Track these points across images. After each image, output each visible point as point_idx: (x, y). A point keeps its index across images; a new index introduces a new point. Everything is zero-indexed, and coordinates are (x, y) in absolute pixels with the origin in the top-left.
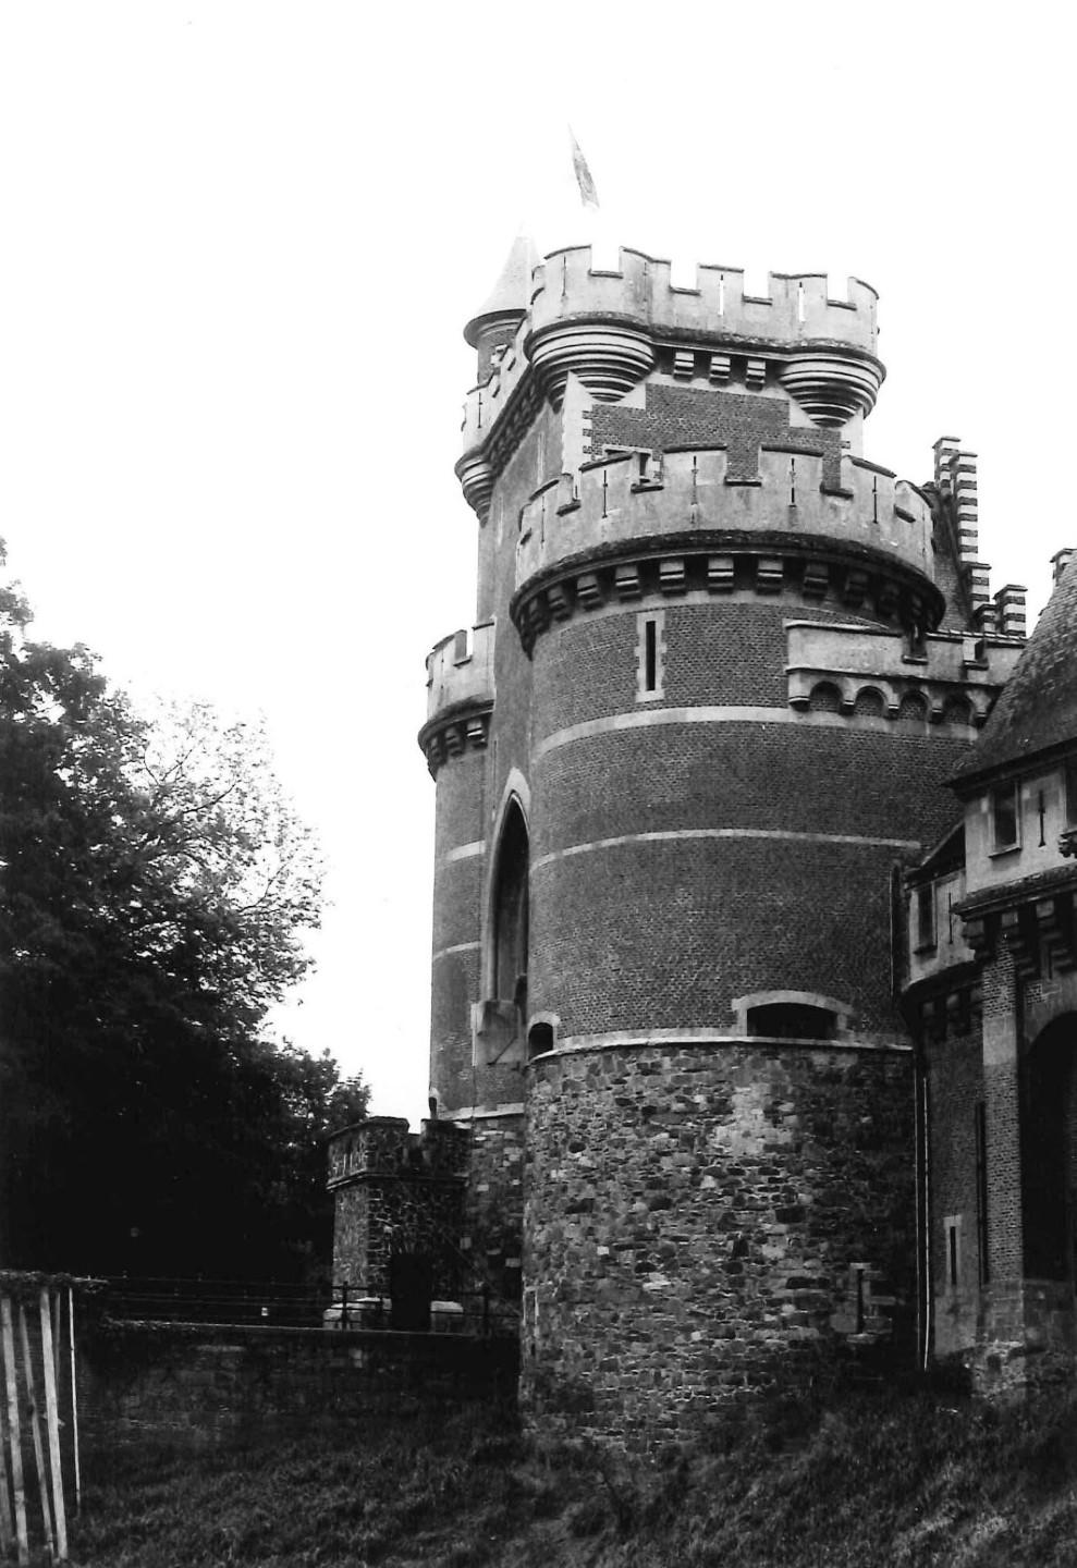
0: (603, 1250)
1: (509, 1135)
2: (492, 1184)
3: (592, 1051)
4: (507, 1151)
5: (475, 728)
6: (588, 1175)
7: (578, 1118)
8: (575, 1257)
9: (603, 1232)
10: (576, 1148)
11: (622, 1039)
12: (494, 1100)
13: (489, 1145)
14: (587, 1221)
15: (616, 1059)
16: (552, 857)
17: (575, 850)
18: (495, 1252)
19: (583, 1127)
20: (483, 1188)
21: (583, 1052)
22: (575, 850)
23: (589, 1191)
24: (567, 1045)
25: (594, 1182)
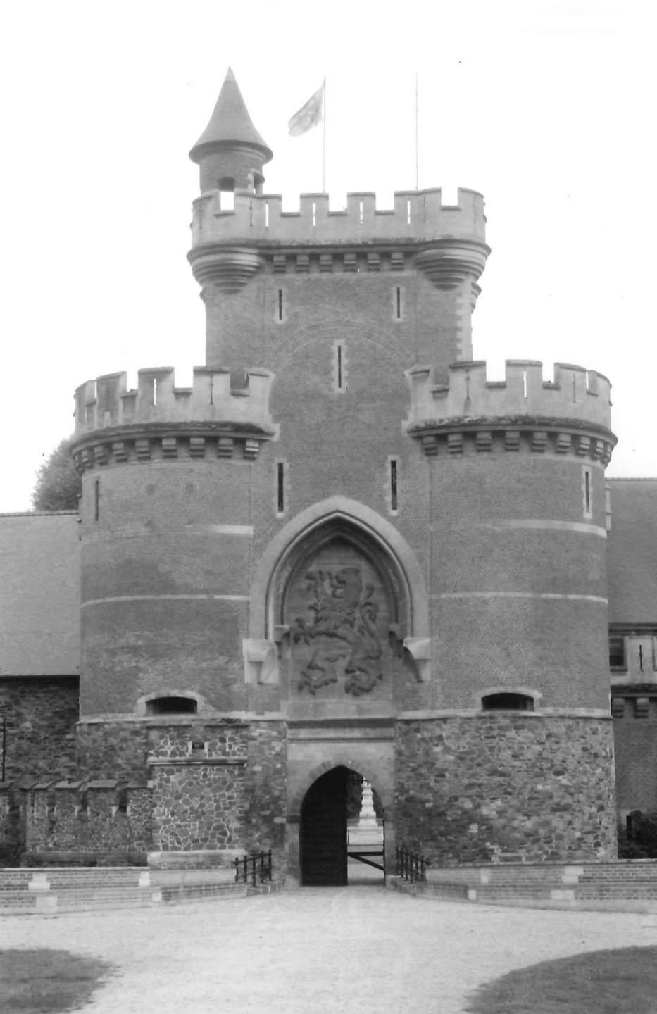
0: (578, 834)
1: (274, 733)
2: (264, 767)
3: (570, 718)
4: (273, 744)
5: (252, 446)
6: (568, 790)
7: (560, 756)
8: (560, 837)
9: (577, 824)
10: (558, 773)
11: (582, 712)
13: (261, 739)
14: (568, 817)
15: (581, 723)
16: (529, 595)
17: (551, 596)
18: (267, 813)
19: (564, 761)
20: (258, 768)
21: (562, 717)
22: (551, 596)
23: (568, 800)
24: (550, 710)
25: (572, 794)
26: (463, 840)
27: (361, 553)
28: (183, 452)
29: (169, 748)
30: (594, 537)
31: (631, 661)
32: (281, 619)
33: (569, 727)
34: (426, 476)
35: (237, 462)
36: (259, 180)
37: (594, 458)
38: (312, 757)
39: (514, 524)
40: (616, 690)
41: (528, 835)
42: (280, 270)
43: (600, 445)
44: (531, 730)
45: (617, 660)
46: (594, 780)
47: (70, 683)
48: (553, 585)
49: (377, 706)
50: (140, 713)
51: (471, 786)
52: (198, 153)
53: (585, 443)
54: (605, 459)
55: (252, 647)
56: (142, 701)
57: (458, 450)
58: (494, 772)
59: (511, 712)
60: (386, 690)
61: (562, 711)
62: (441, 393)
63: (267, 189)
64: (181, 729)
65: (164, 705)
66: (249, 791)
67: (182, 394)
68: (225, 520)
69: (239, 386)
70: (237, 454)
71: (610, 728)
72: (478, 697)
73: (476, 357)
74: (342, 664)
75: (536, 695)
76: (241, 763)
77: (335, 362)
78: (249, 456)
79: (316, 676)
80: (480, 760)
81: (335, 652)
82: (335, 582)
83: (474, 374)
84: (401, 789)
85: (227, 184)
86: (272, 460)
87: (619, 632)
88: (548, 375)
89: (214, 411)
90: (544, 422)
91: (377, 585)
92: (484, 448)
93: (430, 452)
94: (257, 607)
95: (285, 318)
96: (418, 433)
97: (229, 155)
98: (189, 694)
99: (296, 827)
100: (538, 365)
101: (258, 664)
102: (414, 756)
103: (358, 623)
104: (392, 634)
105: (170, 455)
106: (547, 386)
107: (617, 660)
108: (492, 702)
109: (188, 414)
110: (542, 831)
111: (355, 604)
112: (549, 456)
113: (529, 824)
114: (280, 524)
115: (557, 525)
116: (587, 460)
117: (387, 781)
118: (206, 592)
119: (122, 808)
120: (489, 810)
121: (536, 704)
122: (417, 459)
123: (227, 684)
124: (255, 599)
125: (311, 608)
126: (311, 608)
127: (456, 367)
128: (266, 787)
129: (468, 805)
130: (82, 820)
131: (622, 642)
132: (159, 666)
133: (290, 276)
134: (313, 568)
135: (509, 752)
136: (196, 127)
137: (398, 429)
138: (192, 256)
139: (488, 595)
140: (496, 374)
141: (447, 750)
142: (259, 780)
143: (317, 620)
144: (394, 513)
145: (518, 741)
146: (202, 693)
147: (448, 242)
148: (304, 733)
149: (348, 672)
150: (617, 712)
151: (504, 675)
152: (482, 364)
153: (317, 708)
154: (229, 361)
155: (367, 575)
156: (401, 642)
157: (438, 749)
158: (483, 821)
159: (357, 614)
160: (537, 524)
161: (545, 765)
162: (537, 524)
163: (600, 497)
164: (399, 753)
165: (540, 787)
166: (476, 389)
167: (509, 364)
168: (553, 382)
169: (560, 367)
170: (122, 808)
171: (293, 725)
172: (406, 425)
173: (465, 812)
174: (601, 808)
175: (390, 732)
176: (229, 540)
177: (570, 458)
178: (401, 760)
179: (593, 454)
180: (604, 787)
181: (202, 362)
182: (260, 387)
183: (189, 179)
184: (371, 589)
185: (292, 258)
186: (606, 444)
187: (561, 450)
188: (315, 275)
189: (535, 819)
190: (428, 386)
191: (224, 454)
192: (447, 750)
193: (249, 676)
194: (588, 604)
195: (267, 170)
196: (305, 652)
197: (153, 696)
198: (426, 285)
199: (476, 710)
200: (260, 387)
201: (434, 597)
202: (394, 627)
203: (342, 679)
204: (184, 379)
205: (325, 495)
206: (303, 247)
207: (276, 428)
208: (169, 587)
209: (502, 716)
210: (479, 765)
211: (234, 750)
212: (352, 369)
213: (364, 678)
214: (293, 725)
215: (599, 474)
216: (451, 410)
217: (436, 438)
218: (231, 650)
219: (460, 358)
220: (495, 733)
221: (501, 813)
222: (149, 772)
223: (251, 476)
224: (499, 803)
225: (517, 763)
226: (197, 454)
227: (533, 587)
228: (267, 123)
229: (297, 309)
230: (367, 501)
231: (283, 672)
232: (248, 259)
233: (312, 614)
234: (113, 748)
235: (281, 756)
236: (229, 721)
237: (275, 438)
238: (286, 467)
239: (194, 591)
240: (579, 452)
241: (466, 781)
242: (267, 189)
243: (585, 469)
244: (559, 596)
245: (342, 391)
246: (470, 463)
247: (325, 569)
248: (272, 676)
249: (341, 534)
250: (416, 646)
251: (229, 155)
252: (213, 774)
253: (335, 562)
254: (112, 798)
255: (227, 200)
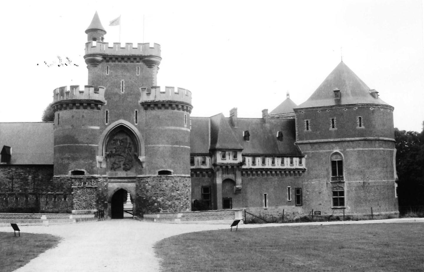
0: (182, 205)
1: (105, 180)
2: (102, 189)
3: (180, 177)
4: (105, 183)
6: (179, 195)
7: (177, 186)
8: (177, 206)
9: (182, 203)
11: (183, 175)
12: (101, 174)
13: (101, 182)
14: (179, 201)
15: (183, 178)
16: (171, 146)
17: (176, 146)
18: (103, 200)
19: (179, 187)
20: (100, 189)
21: (178, 177)
22: (176, 146)
23: (179, 197)
24: (175, 175)
25: (180, 196)
26: (153, 207)
27: (127, 134)
28: (81, 107)
29: (77, 184)
30: (187, 131)
31: (196, 163)
32: (106, 151)
33: (180, 179)
34: (144, 115)
35: (96, 110)
36: (103, 39)
37: (187, 112)
38: (114, 186)
39: (167, 128)
40: (192, 170)
41: (169, 206)
42: (108, 61)
43: (189, 108)
44: (170, 180)
45: (192, 162)
46: (186, 192)
47: (51, 167)
48: (177, 143)
49: (131, 174)
50: (69, 175)
51: (155, 194)
52: (87, 31)
53: (185, 108)
54: (190, 112)
55: (99, 158)
56: (70, 172)
57: (153, 108)
58: (161, 190)
59: (165, 175)
60: (134, 169)
61: (178, 175)
62: (149, 94)
63: (105, 41)
64: (80, 179)
65: (75, 173)
66: (98, 195)
67: (81, 92)
68: (92, 125)
69: (96, 91)
70: (95, 108)
71: (190, 179)
72: (157, 171)
73: (158, 85)
74: (122, 163)
75: (172, 171)
76: (96, 188)
77: (121, 85)
78: (99, 109)
79: (115, 166)
80: (157, 187)
81: (120, 160)
82: (121, 142)
83: (157, 89)
84: (137, 195)
85: (95, 39)
86: (105, 110)
87: (193, 156)
88: (176, 90)
89: (90, 97)
90: (175, 102)
91: (132, 143)
92: (160, 108)
93: (146, 109)
94: (100, 148)
95: (109, 73)
96: (143, 104)
97: (95, 33)
98: (83, 170)
99: (110, 204)
100: (173, 88)
101: (100, 163)
102: (140, 186)
103: (127, 152)
104: (135, 155)
105: (78, 108)
106: (176, 93)
107: (192, 162)
108: (161, 173)
109: (83, 97)
110: (173, 205)
111: (126, 147)
112: (176, 111)
113: (170, 203)
114: (106, 126)
115: (178, 128)
116: (185, 112)
117: (133, 192)
118: (87, 143)
119: (65, 199)
120: (160, 200)
121: (172, 173)
122: (142, 110)
123: (92, 167)
124: (100, 146)
125: (114, 148)
126: (114, 148)
127: (152, 87)
128: (102, 193)
129: (154, 198)
130: (55, 202)
131: (193, 158)
132: (74, 163)
133: (110, 63)
134: (115, 138)
135: (165, 185)
136: (87, 25)
137: (138, 103)
138: (85, 57)
139: (160, 145)
140: (163, 89)
141: (149, 185)
142: (100, 192)
143: (116, 151)
144: (136, 124)
145: (167, 183)
146: (85, 170)
147: (151, 56)
148: (112, 180)
149: (124, 165)
150: (192, 175)
151: (164, 166)
152: (159, 87)
153: (116, 174)
154: (94, 85)
155: (129, 140)
156: (138, 157)
157: (147, 185)
158: (158, 202)
159: (126, 150)
160: (173, 128)
161: (174, 188)
162: (173, 128)
163: (188, 121)
164: (137, 185)
165: (172, 194)
166: (158, 93)
167: (167, 87)
168: (177, 92)
169: (179, 88)
170: (65, 199)
171: (109, 178)
172: (140, 102)
173: (153, 200)
174: (188, 199)
175: (135, 180)
176: (93, 130)
177: (181, 111)
178: (137, 188)
179: (187, 110)
180: (188, 194)
181: (87, 84)
182: (102, 91)
183: (85, 38)
184: (130, 144)
185: (111, 58)
186: (190, 108)
187: (179, 109)
188: (117, 63)
189: (171, 202)
190: (145, 92)
191: (92, 108)
192: (149, 185)
193: (98, 165)
194: (185, 148)
195: (105, 36)
196: (113, 159)
197: (73, 170)
198: (145, 67)
199: (157, 175)
200: (102, 91)
201: (146, 146)
202: (136, 154)
203: (122, 167)
204: (82, 88)
205: (118, 119)
206: (114, 56)
207: (106, 101)
208: (77, 142)
209: (163, 176)
210: (157, 188)
211: (94, 185)
212: (126, 87)
213: (128, 166)
214: (109, 178)
215: (188, 116)
216: (151, 98)
217: (147, 106)
218: (93, 158)
219: (154, 85)
220: (161, 180)
221: (163, 200)
222: (72, 190)
223: (99, 114)
224: (162, 198)
225: (167, 188)
226: (85, 108)
227: (173, 144)
228: (105, 25)
229: (112, 71)
230: (129, 121)
231: (107, 165)
232: (100, 58)
233: (114, 150)
234: (63, 183)
235: (106, 186)
236: (93, 177)
237: (106, 104)
238: (108, 111)
239: (83, 143)
240: (183, 110)
241: (154, 193)
242: (105, 41)
243: (185, 114)
244: (178, 146)
245: (123, 93)
246: (156, 112)
247: (117, 138)
248: (104, 166)
249: (122, 130)
250: (142, 158)
251: (95, 33)
252: (89, 190)
253: (121, 137)
254: (62, 196)
255: (94, 43)
